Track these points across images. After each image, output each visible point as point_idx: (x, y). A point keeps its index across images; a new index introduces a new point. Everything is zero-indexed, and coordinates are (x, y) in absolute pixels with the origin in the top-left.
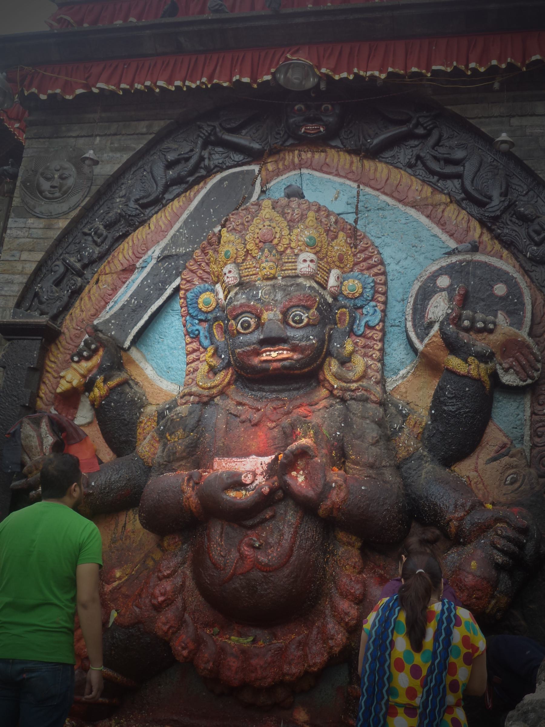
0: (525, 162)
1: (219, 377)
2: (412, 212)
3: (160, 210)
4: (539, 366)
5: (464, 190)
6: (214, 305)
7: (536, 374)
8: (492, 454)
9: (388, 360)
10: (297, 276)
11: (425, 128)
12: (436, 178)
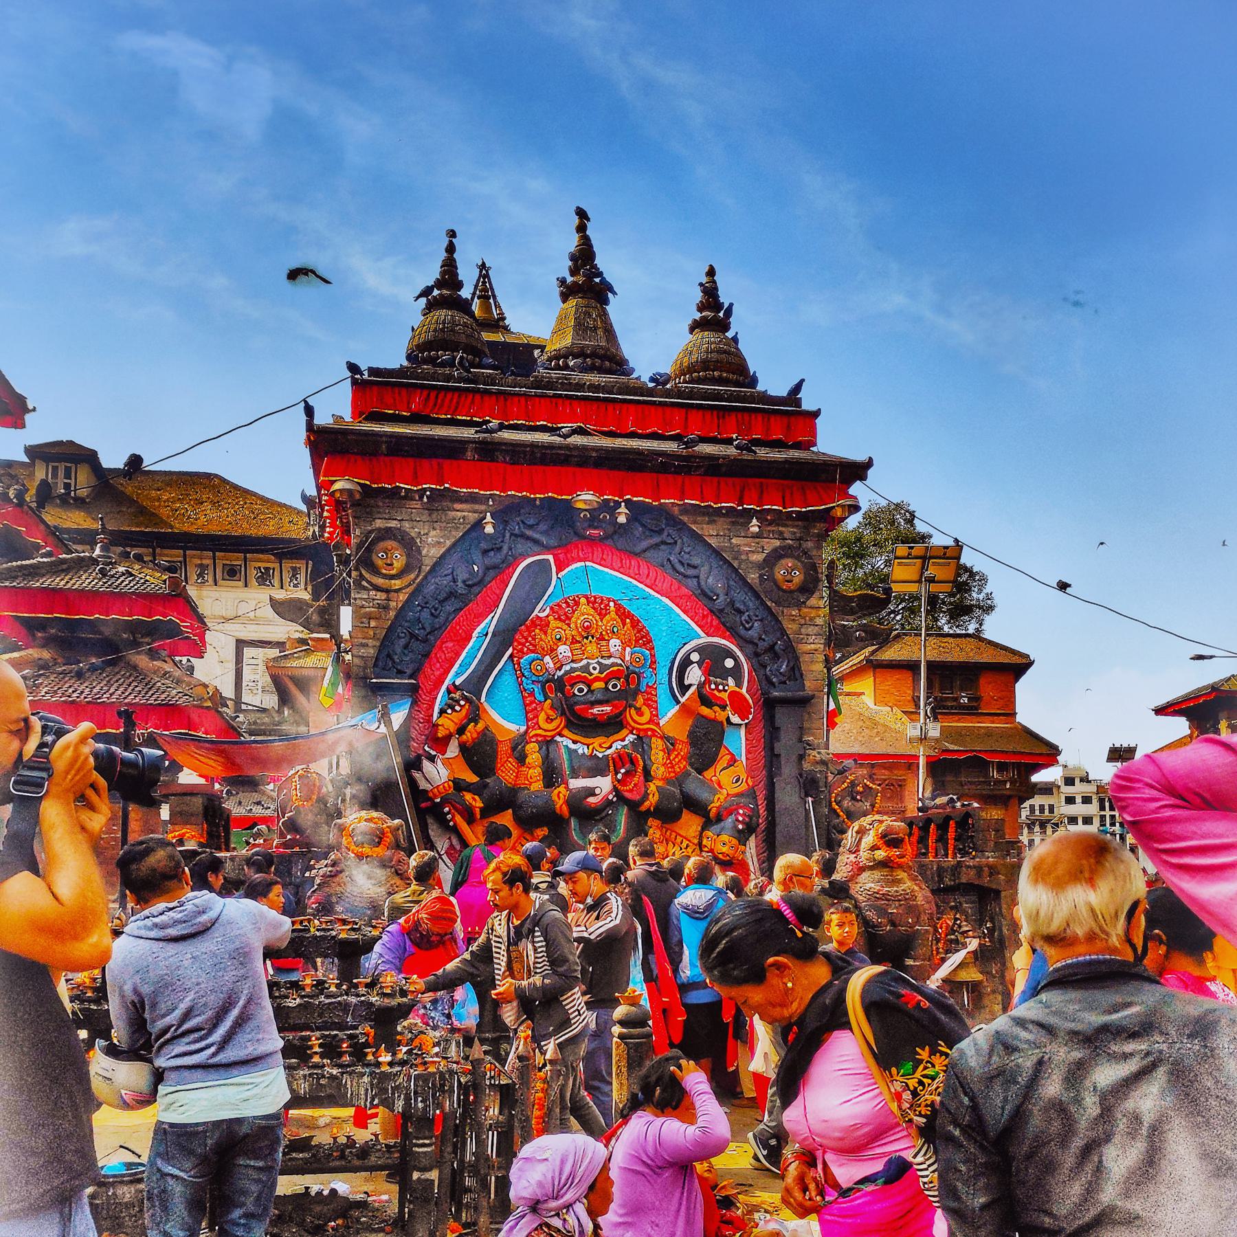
1: (554, 724)
2: (667, 601)
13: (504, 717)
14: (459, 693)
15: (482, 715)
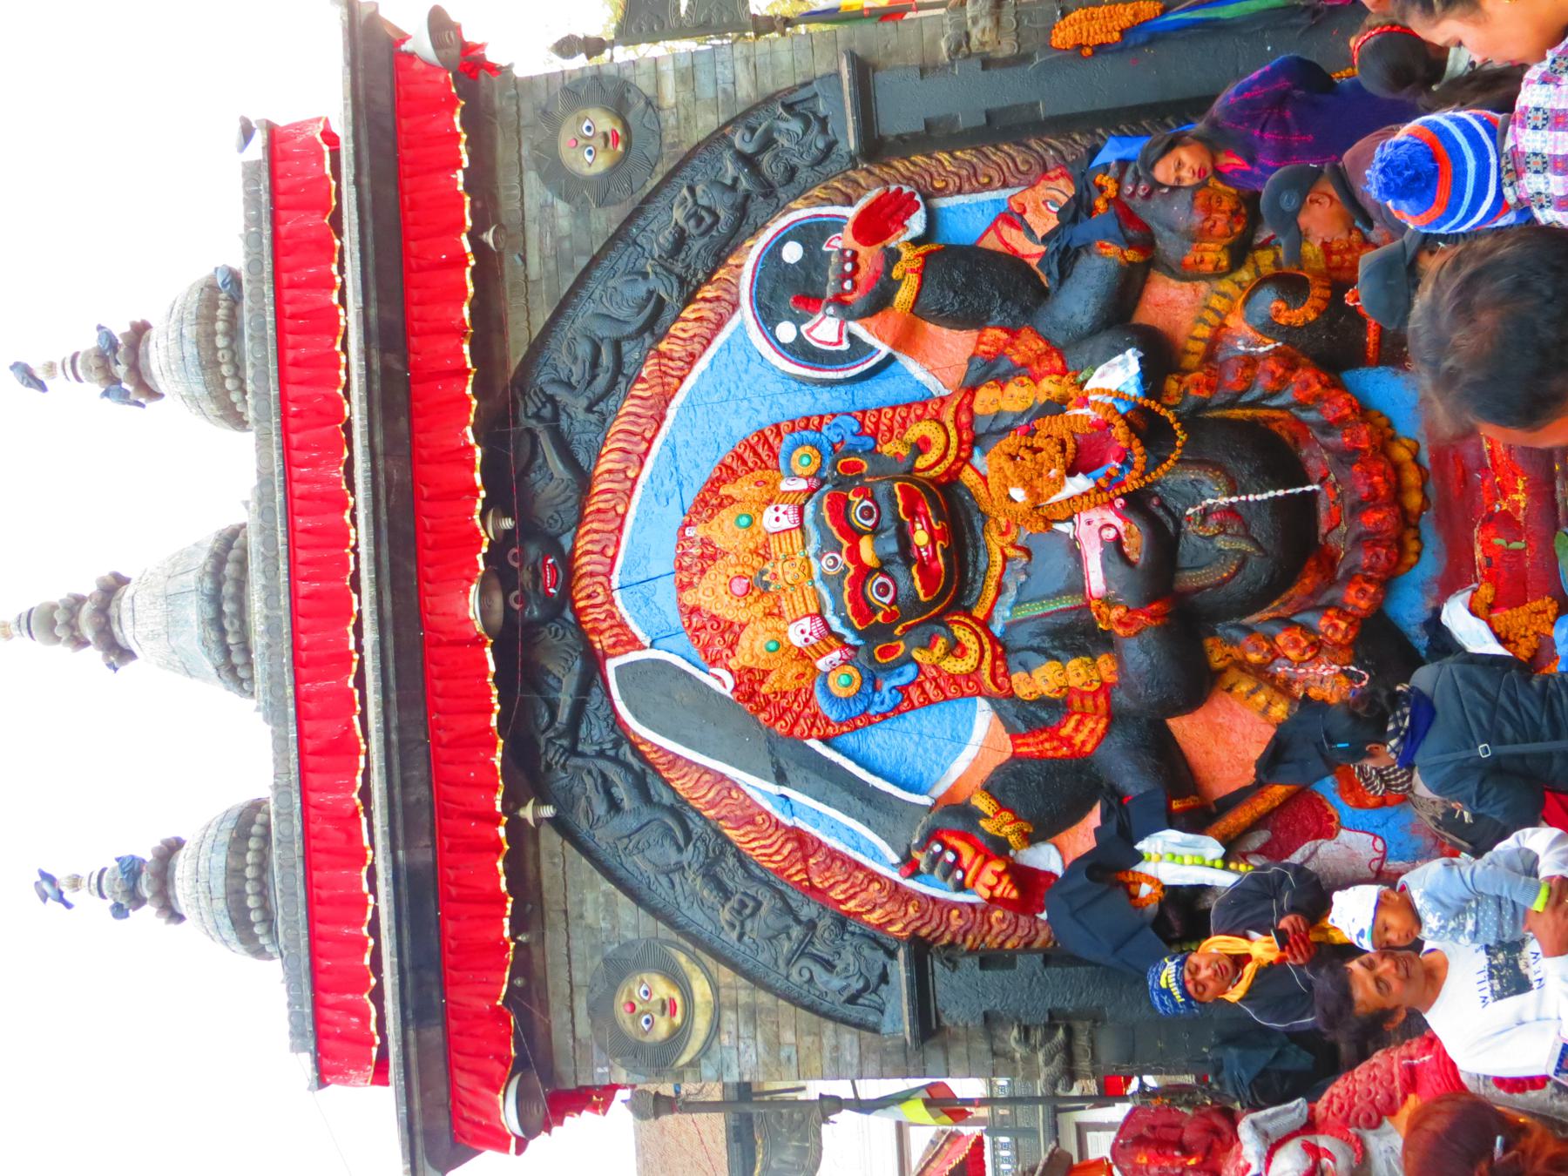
0: (595, 251)
2: (674, 404)
3: (693, 809)
4: (893, 188)
5: (640, 332)
6: (849, 669)
7: (906, 190)
8: (1022, 234)
9: (907, 398)
10: (801, 526)
11: (544, 405)
12: (620, 378)
13: (964, 746)
14: (916, 855)
15: (961, 799)
